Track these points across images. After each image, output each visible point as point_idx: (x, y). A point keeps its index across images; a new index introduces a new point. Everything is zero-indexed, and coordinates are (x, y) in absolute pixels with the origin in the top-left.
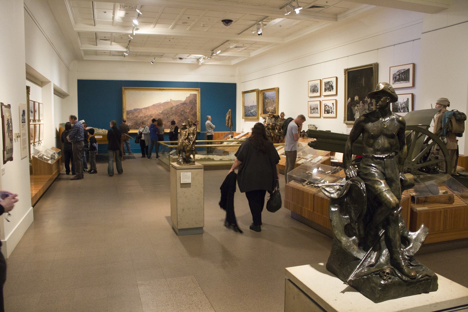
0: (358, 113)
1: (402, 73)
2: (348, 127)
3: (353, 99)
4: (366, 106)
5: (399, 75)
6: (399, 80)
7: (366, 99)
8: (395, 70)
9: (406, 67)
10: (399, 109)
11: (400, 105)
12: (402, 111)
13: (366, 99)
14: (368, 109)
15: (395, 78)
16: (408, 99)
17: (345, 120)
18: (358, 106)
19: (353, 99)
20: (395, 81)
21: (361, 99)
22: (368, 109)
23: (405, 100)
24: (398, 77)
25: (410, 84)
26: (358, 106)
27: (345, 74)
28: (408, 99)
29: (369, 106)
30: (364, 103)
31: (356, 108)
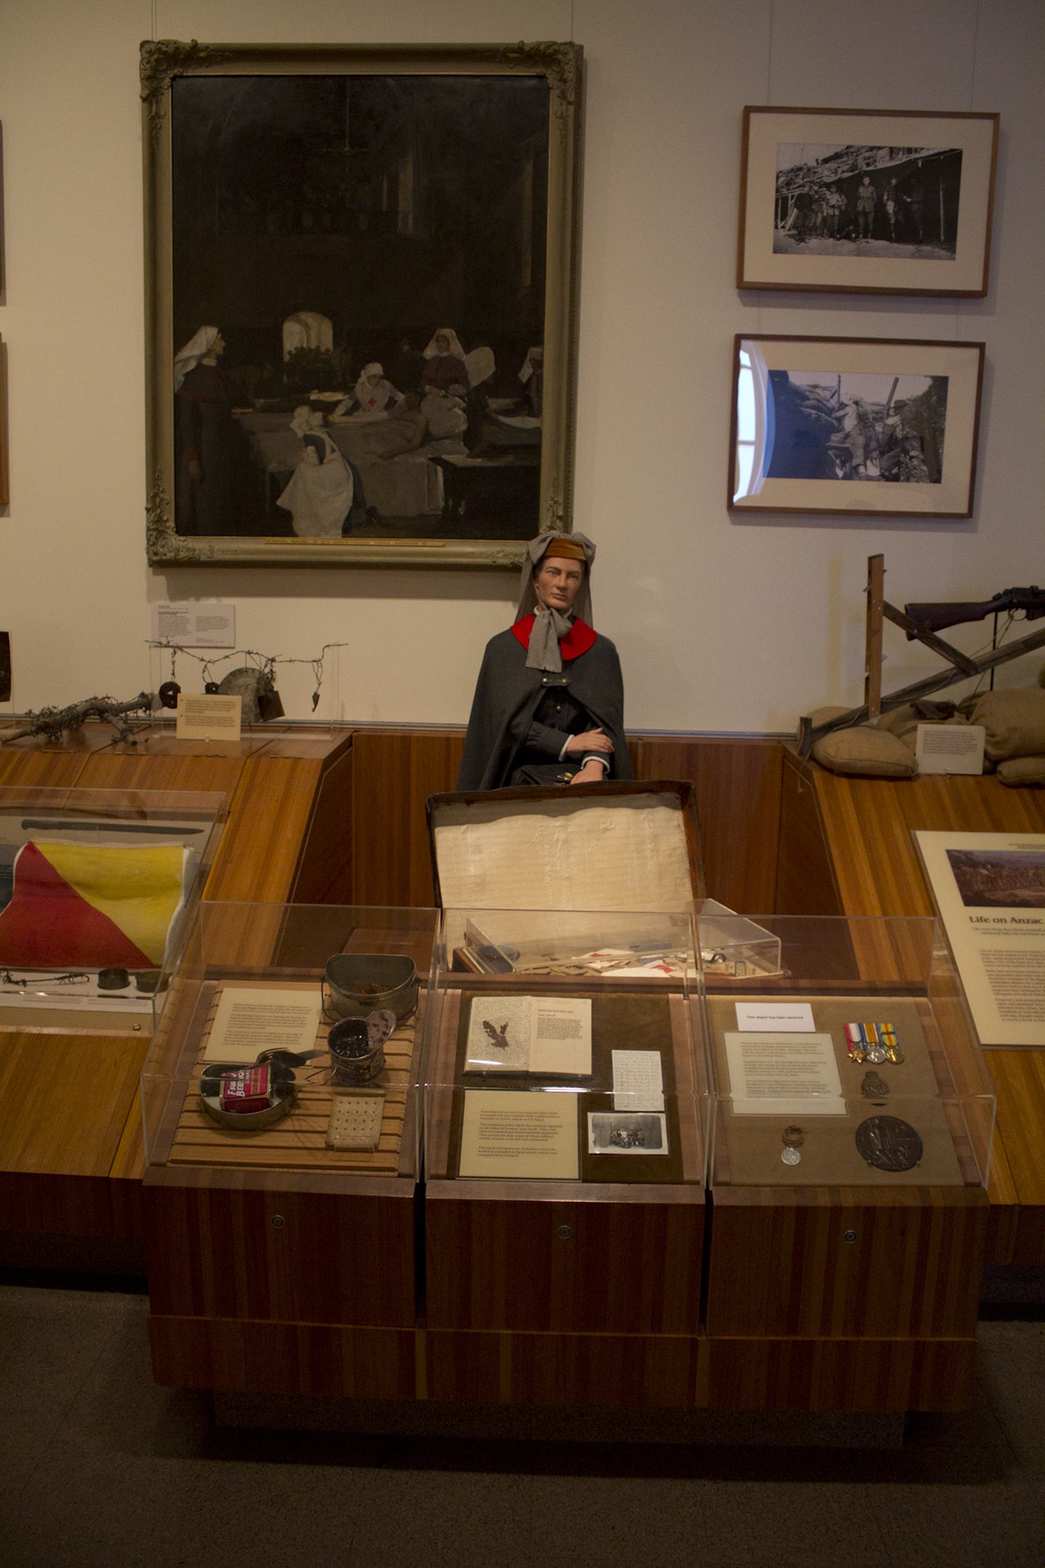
0: (336, 468)
1: (879, 177)
2: (176, 594)
3: (252, 344)
4: (447, 413)
5: (847, 186)
6: (848, 228)
7: (445, 345)
8: (785, 145)
9: (930, 138)
10: (846, 456)
11: (850, 423)
12: (873, 470)
13: (445, 345)
14: (470, 438)
15: (805, 203)
16: (940, 384)
17: (156, 531)
18: (316, 406)
19: (252, 344)
20: (802, 233)
21: (360, 343)
22: (470, 438)
23: (913, 388)
24: (834, 198)
25: (959, 271)
26: (328, 408)
27: (151, 97)
28: (940, 384)
29: (476, 412)
30: (409, 377)
31: (304, 421)
